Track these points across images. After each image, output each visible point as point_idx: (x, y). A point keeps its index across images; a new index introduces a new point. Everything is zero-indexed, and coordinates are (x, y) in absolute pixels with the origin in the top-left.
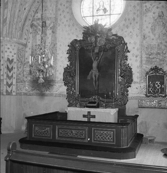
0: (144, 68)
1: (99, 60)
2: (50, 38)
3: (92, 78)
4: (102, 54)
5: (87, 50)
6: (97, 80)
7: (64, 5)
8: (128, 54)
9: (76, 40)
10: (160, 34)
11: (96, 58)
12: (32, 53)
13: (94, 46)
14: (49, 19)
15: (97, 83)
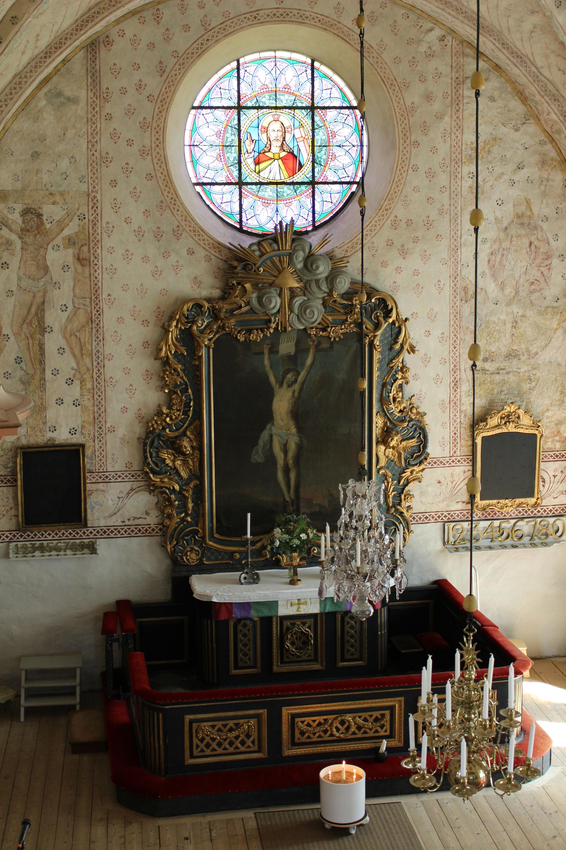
0: (463, 408)
1: (297, 387)
3: (271, 458)
4: (309, 361)
6: (291, 462)
7: (130, 143)
9: (198, 306)
10: (522, 281)
11: (284, 377)
13: (276, 329)
14: (58, 198)
15: (293, 475)
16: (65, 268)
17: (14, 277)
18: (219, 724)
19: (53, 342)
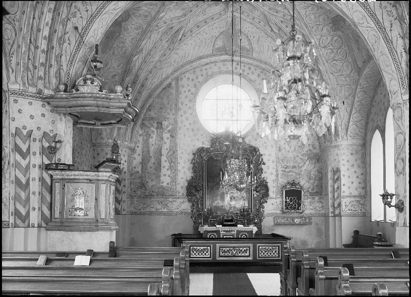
2: (168, 142)
5: (217, 160)
8: (263, 166)
12: (142, 160)
16: (168, 138)
17: (154, 140)
18: (198, 248)
19: (164, 158)
